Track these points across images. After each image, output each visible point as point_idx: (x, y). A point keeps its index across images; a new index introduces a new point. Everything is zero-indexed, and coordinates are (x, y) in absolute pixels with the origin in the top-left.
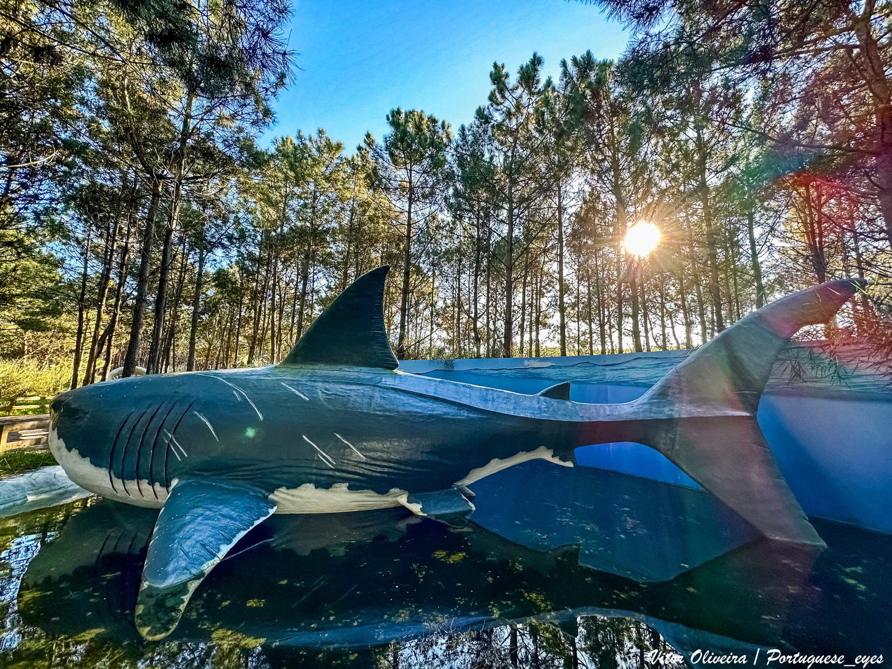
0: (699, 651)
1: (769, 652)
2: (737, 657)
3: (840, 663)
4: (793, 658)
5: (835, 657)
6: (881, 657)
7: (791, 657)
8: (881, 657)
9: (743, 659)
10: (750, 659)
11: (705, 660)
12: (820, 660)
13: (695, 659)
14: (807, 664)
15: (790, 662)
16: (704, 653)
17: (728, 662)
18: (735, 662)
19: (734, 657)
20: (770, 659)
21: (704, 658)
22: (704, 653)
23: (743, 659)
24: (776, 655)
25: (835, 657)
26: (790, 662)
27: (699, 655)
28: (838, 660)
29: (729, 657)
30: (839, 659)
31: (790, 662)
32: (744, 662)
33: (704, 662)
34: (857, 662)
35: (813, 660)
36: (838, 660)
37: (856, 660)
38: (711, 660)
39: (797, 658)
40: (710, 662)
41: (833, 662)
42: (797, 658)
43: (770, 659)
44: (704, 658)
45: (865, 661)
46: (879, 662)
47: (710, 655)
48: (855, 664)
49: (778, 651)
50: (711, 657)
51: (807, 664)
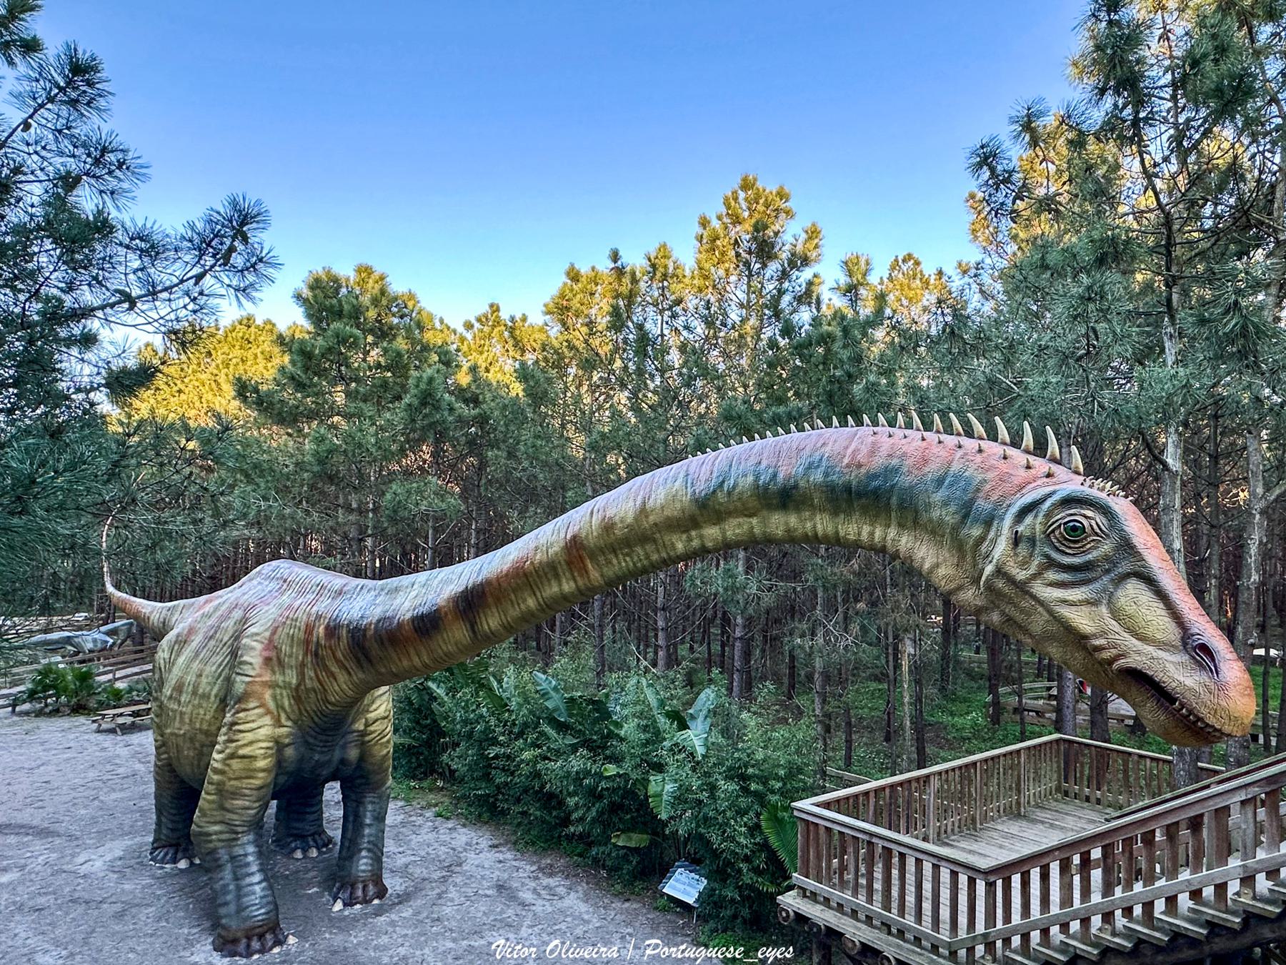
1: (648, 942)
2: (605, 949)
3: (738, 956)
4: (678, 950)
5: (732, 949)
6: (791, 949)
7: (675, 949)
11: (567, 951)
13: (552, 952)
14: (696, 959)
15: (674, 956)
16: (563, 943)
17: (595, 956)
19: (602, 949)
20: (649, 952)
21: (564, 951)
24: (657, 946)
25: (732, 949)
27: (557, 946)
29: (596, 950)
30: (737, 952)
31: (674, 956)
33: (564, 956)
37: (760, 952)
38: (573, 953)
39: (683, 951)
40: (571, 956)
41: (729, 956)
42: (683, 951)
43: (649, 952)
44: (564, 951)
45: (772, 954)
46: (788, 956)
49: (659, 942)
50: (572, 950)
51: (696, 959)
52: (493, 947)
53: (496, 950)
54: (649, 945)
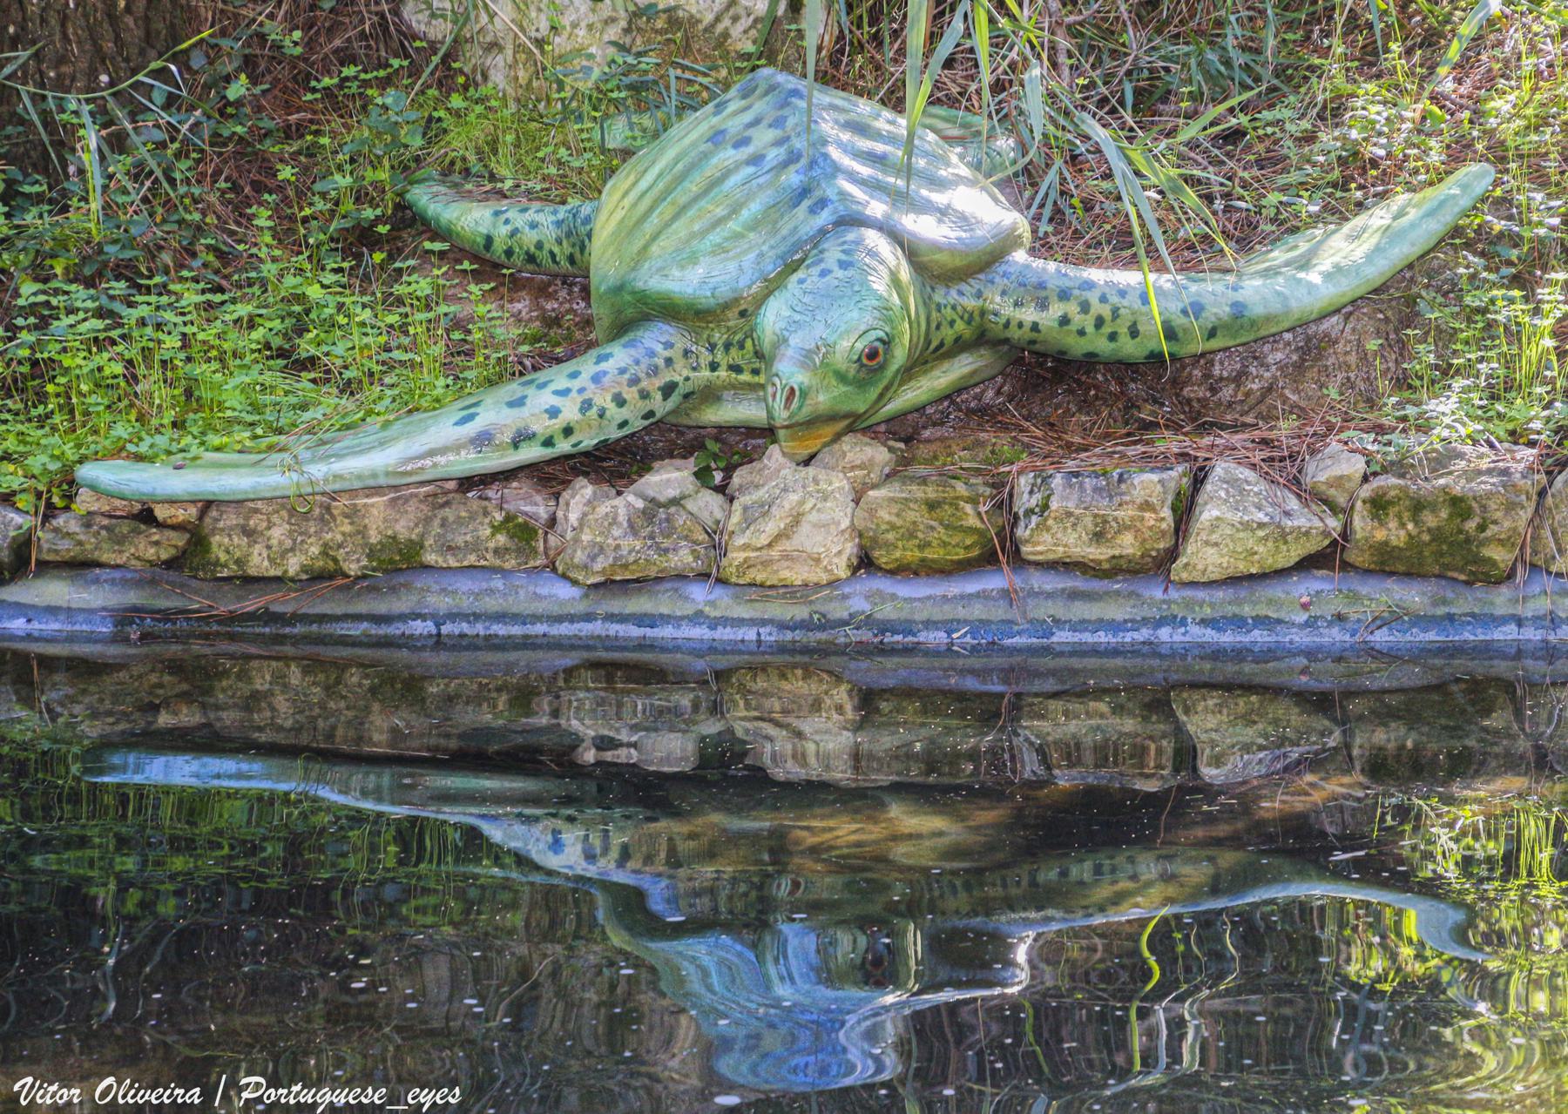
0: (110, 1080)
5: (370, 1090)
6: (457, 1090)
7: (285, 1091)
8: (457, 1090)
9: (195, 1096)
10: (208, 1095)
11: (124, 1096)
12: (341, 1098)
13: (104, 1095)
14: (315, 1105)
16: (120, 1083)
17: (167, 1101)
18: (180, 1101)
19: (177, 1091)
22: (120, 1083)
23: (195, 1096)
24: (258, 1085)
25: (370, 1090)
26: (283, 1101)
27: (110, 1087)
28: (374, 1096)
31: (283, 1101)
32: (197, 1101)
33: (121, 1101)
34: (411, 1101)
35: (326, 1097)
36: (374, 1096)
41: (365, 1101)
43: (245, 1095)
45: (427, 1098)
47: (131, 1087)
48: (407, 1103)
51: (315, 1105)
52: (16, 1088)
53: (19, 1093)
54: (248, 1085)
